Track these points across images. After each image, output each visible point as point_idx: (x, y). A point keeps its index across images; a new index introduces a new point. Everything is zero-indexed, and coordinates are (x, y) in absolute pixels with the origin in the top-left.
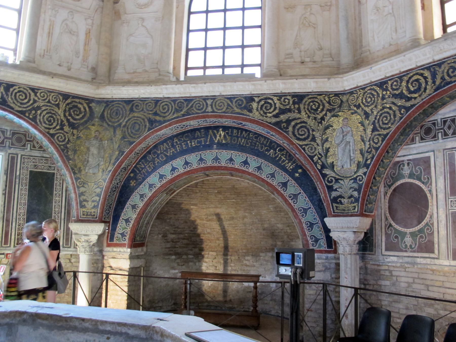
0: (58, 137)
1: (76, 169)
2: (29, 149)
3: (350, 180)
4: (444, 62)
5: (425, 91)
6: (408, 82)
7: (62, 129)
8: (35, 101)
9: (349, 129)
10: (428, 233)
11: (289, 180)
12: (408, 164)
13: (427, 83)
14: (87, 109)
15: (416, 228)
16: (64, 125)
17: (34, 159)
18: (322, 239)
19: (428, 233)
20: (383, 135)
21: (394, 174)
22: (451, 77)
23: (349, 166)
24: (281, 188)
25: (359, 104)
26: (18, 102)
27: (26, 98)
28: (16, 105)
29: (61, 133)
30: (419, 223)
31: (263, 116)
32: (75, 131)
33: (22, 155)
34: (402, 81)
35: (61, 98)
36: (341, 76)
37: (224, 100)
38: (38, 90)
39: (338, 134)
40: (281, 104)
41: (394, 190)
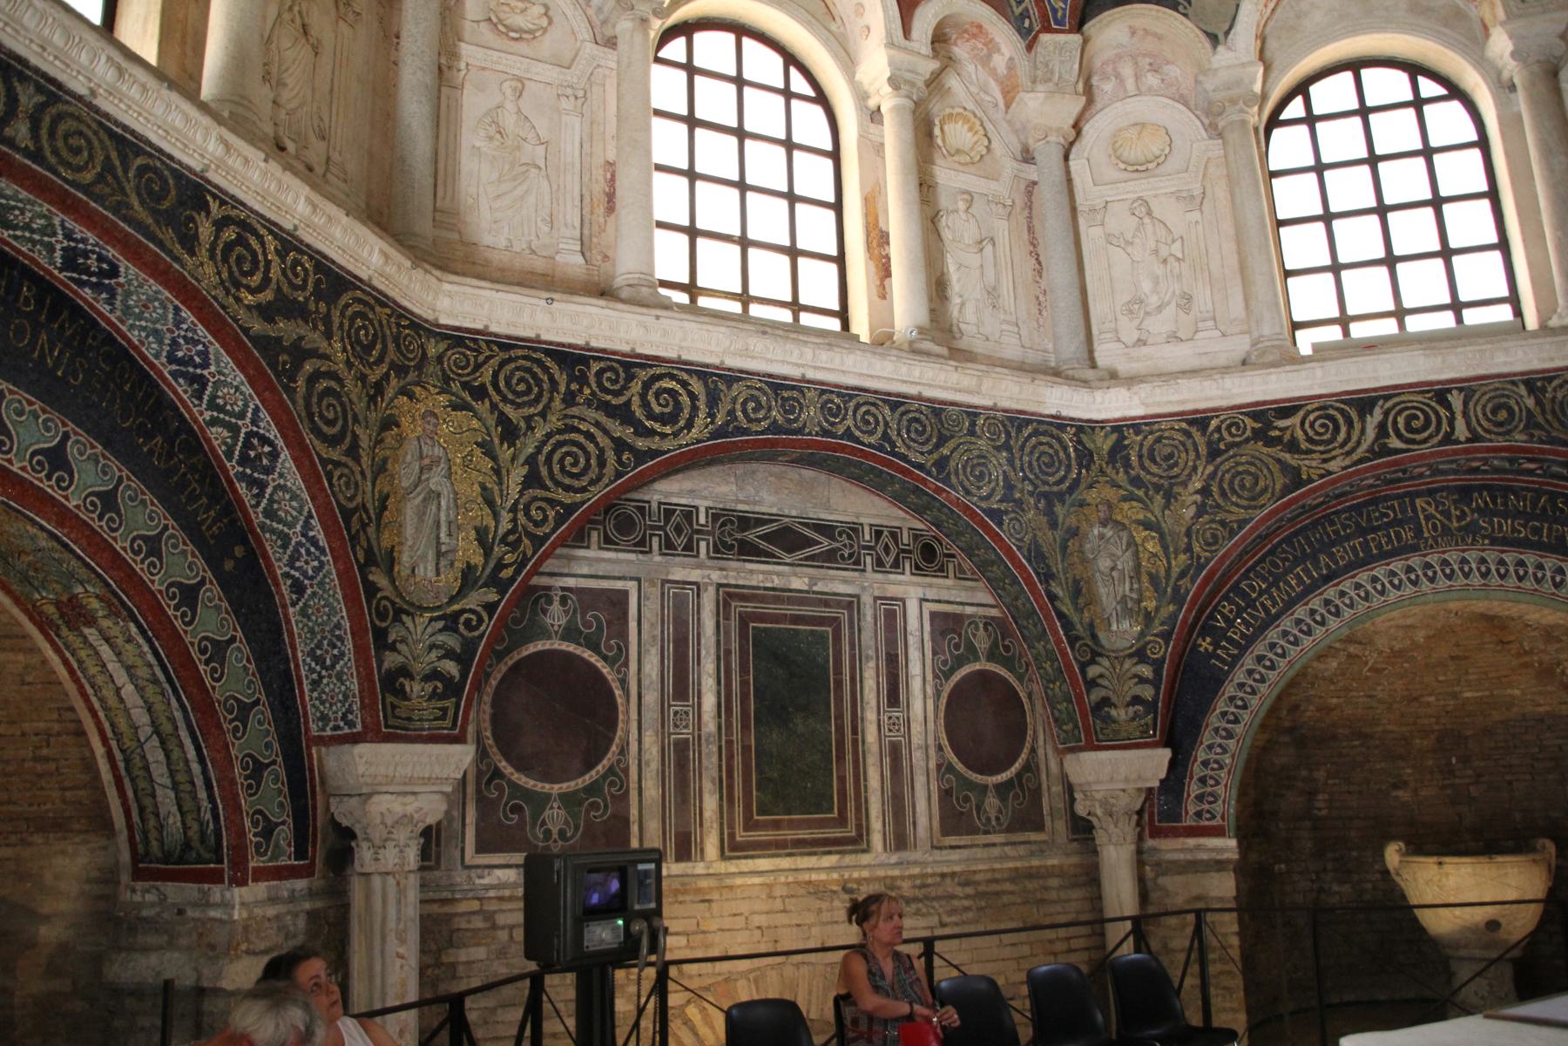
3: (432, 620)
4: (741, 379)
5: (689, 425)
6: (647, 386)
9: (438, 451)
10: (613, 796)
11: (202, 582)
12: (564, 601)
13: (695, 408)
15: (580, 781)
18: (283, 823)
19: (613, 796)
20: (560, 503)
21: (517, 621)
22: (750, 420)
23: (431, 574)
24: (177, 608)
25: (483, 386)
30: (589, 766)
31: (228, 292)
34: (631, 377)
36: (438, 273)
37: (96, 133)
39: (409, 458)
40: (284, 272)
41: (515, 668)
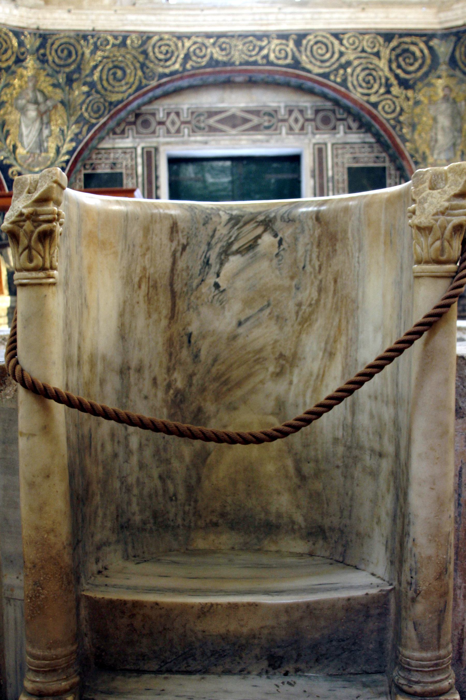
0: (383, 108)
1: (417, 156)
2: (342, 133)
7: (388, 92)
8: (341, 54)
14: (426, 51)
16: (391, 85)
17: (351, 148)
26: (316, 59)
27: (327, 51)
28: (315, 65)
29: (386, 99)
32: (410, 93)
33: (333, 145)
35: (381, 40)
38: (343, 34)
